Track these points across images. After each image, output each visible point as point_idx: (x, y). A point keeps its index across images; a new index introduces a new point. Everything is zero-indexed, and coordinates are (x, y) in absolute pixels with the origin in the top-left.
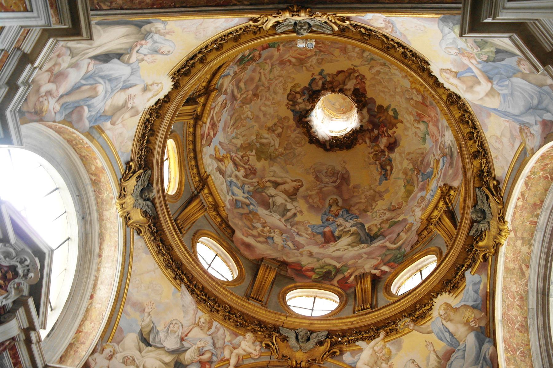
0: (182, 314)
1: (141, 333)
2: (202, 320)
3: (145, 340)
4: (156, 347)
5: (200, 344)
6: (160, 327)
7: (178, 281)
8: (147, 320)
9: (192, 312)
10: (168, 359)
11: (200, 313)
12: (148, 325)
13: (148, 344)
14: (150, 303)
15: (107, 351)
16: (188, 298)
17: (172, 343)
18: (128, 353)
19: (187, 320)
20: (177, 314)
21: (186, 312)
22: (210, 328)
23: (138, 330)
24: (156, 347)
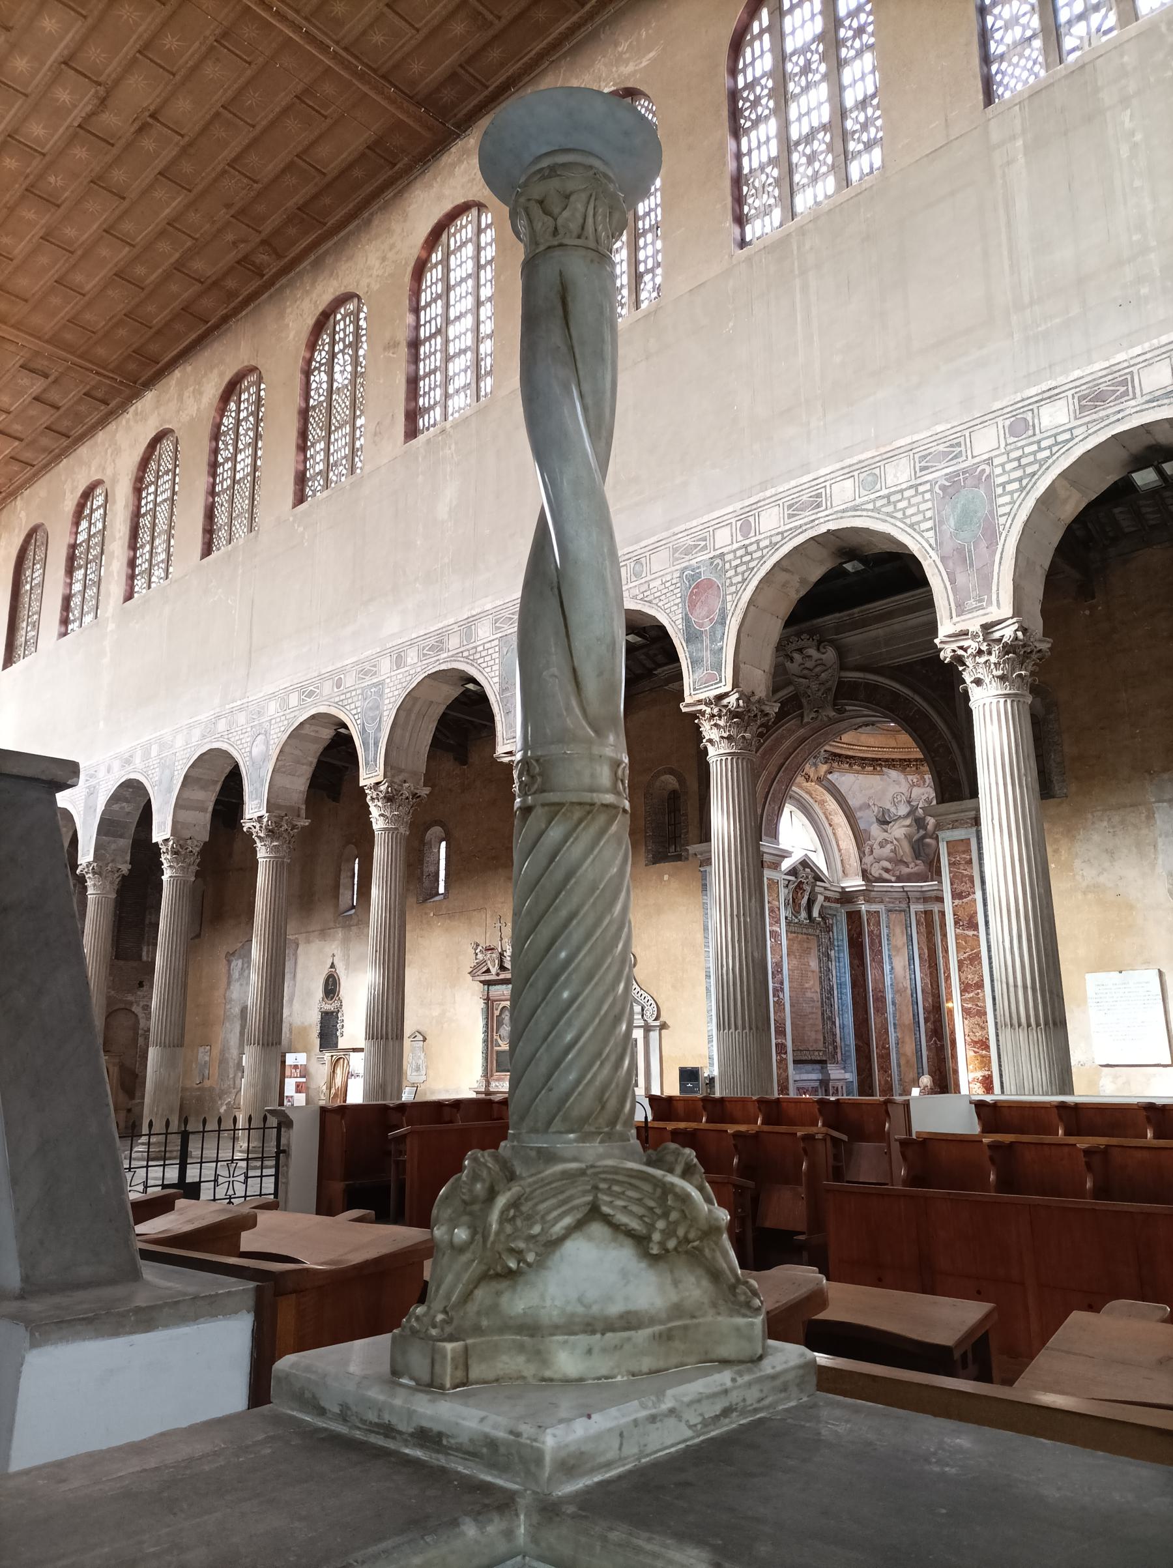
0: (897, 787)
1: (878, 820)
2: (915, 780)
3: (883, 822)
4: (894, 820)
5: (924, 797)
6: (888, 806)
7: (878, 768)
8: (876, 809)
9: (903, 780)
10: (908, 822)
11: (910, 777)
12: (879, 812)
13: (888, 823)
14: (870, 798)
15: (867, 850)
16: (893, 774)
17: (903, 810)
18: (879, 839)
19: (904, 788)
20: (893, 789)
21: (899, 783)
22: (924, 782)
23: (875, 820)
24: (894, 820)
